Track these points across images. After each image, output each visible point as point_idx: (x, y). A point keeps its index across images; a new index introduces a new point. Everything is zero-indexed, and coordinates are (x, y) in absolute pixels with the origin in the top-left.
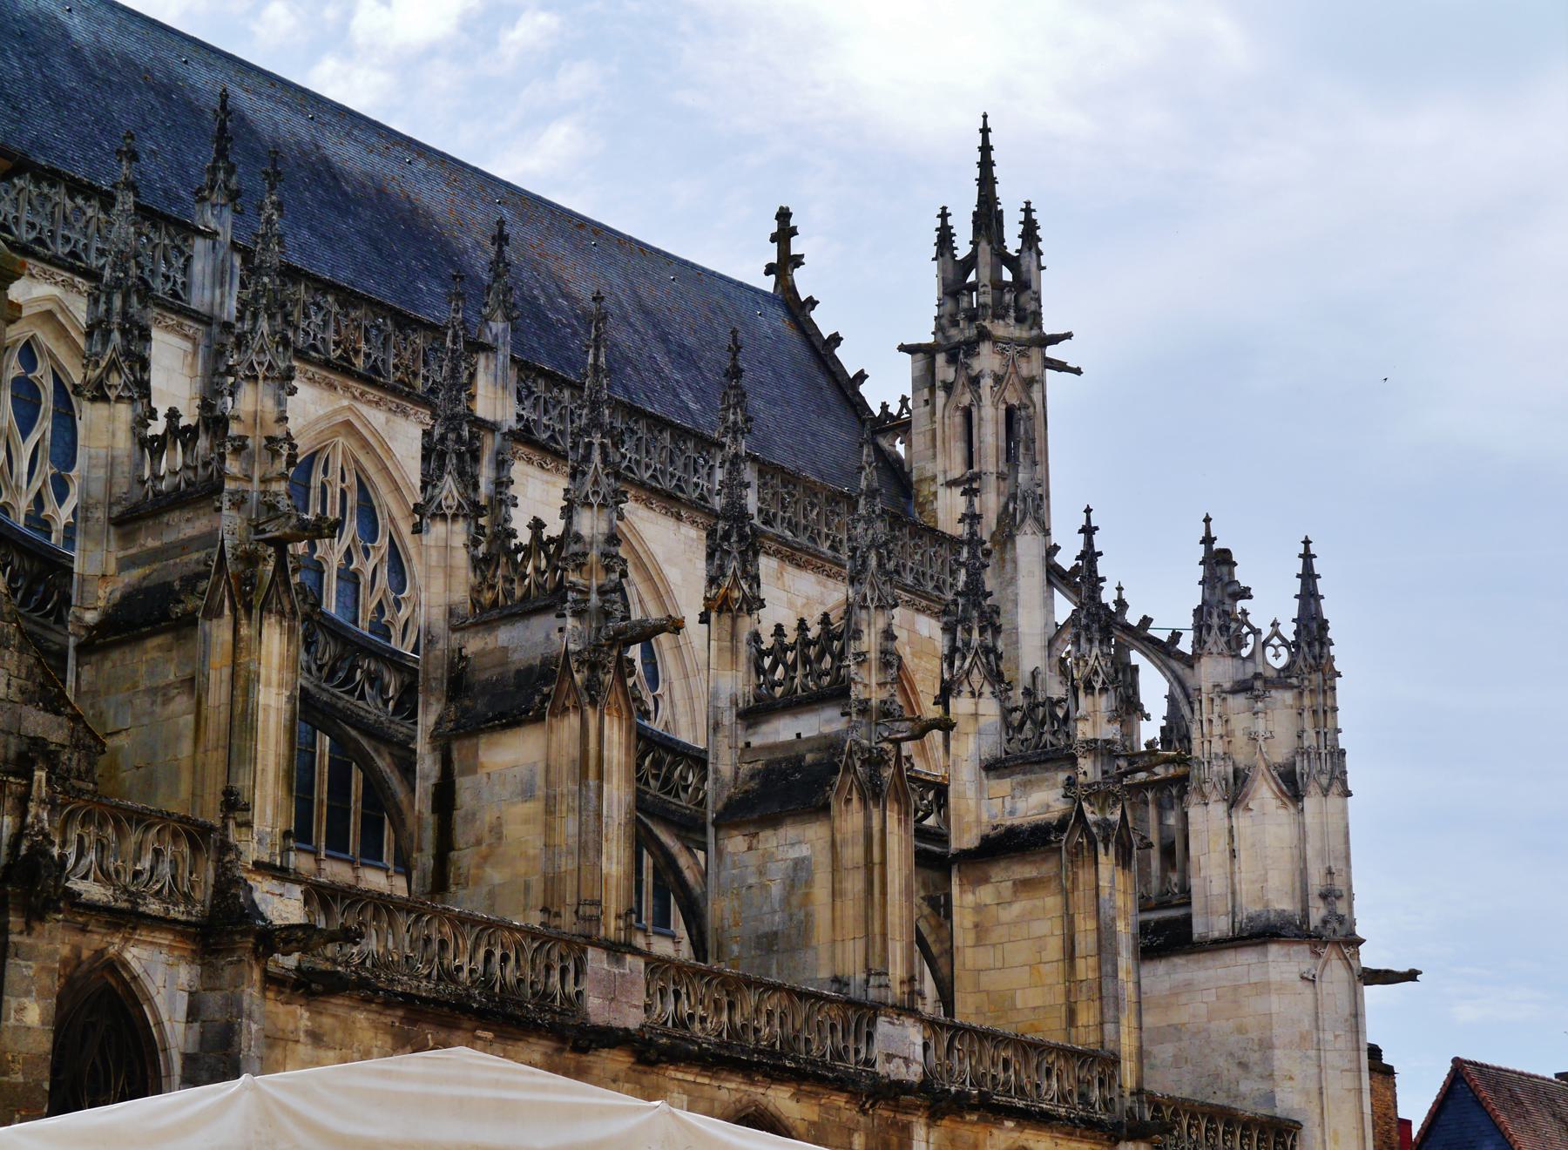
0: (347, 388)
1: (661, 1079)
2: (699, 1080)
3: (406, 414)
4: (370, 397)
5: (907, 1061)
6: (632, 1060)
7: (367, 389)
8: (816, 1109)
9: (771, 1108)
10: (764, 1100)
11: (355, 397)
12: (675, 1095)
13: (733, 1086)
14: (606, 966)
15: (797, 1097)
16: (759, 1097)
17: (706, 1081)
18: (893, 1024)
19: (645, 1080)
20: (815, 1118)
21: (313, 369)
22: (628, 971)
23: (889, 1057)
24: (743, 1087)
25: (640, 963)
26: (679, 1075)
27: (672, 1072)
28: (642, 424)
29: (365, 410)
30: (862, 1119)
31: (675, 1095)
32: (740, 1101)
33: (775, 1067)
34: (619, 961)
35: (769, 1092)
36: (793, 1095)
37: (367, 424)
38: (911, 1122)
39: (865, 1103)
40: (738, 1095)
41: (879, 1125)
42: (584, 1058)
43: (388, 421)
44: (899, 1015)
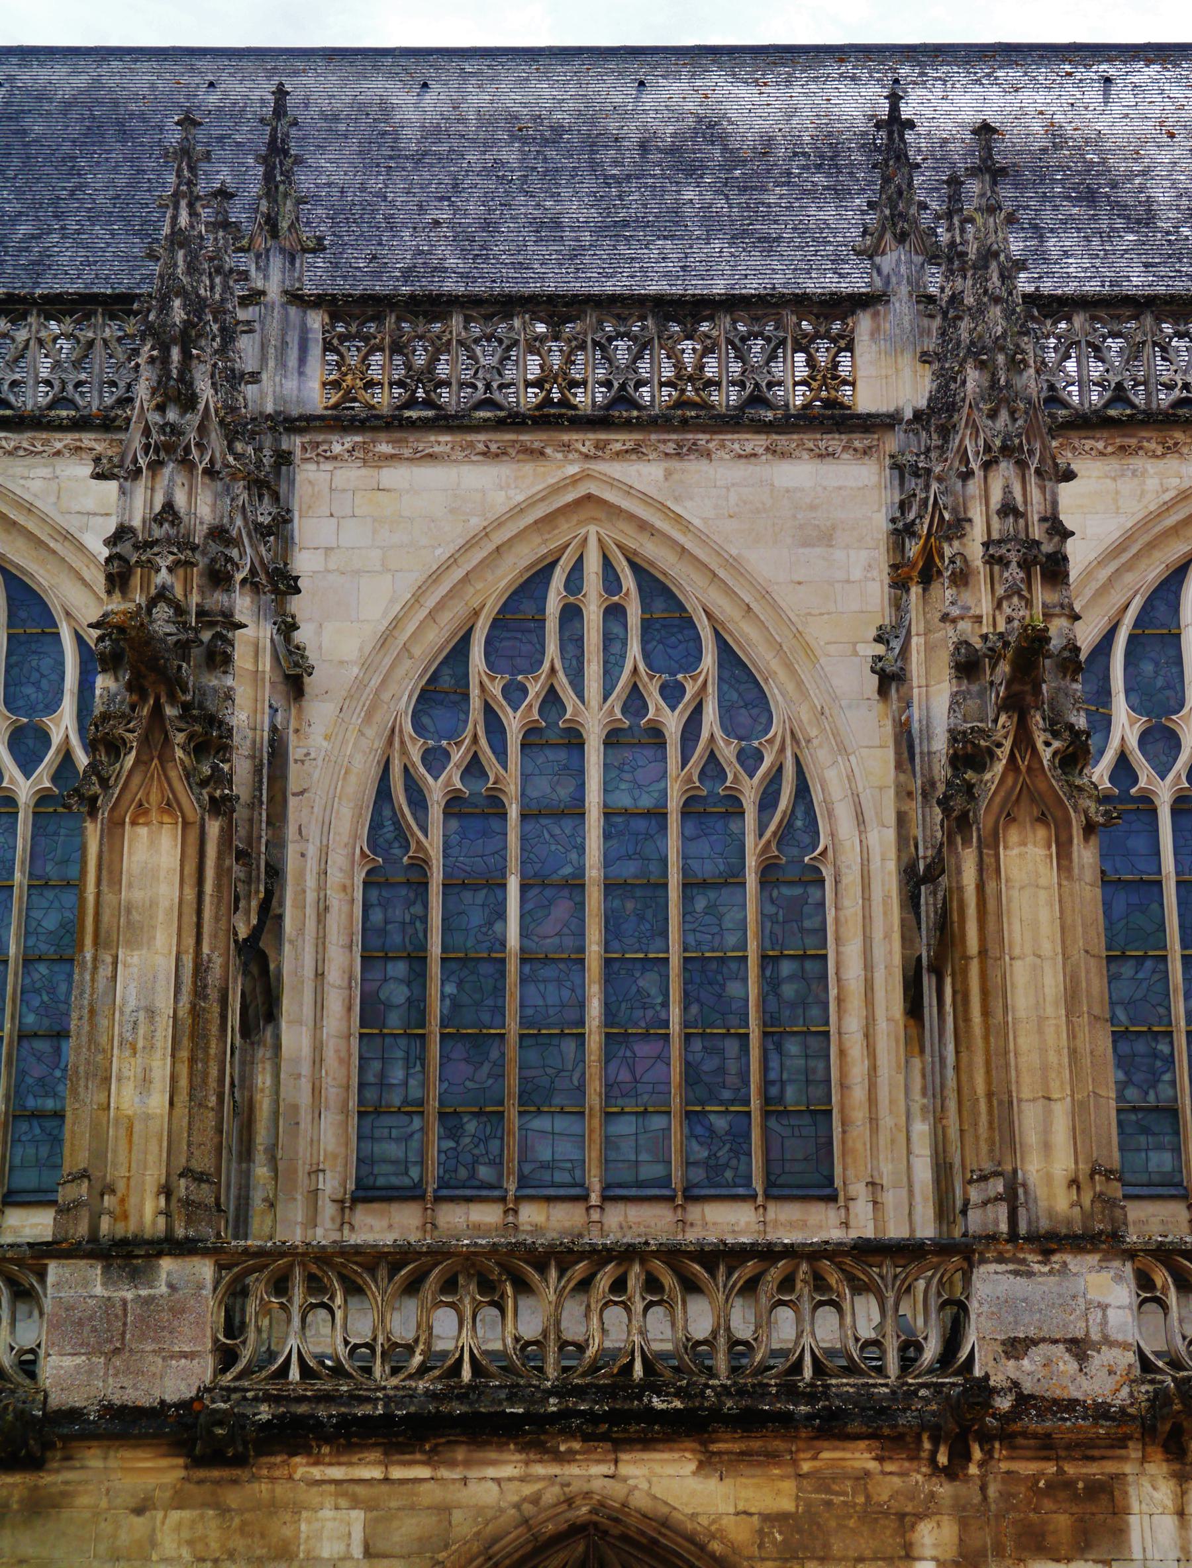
0: (567, 447)
1: (280, 1489)
2: (397, 1473)
3: (785, 455)
4: (618, 447)
5: (1079, 1348)
6: (181, 1461)
7: (603, 436)
8: (789, 1486)
9: (639, 1501)
10: (617, 1490)
11: (587, 457)
12: (327, 1513)
13: (507, 1471)
14: (99, 1290)
15: (708, 1463)
16: (597, 1485)
17: (423, 1472)
18: (1030, 1274)
19: (232, 1498)
20: (787, 1505)
21: (482, 437)
22: (164, 1289)
23: (1016, 1347)
24: (540, 1470)
25: (205, 1269)
26: (337, 1473)
27: (302, 1468)
28: (1079, 320)
29: (616, 470)
30: (945, 1490)
31: (327, 1513)
32: (535, 1500)
33: (615, 1417)
34: (136, 1276)
35: (624, 1470)
36: (701, 1465)
37: (629, 490)
38: (1120, 1477)
39: (934, 1453)
40: (528, 1490)
41: (1005, 1496)
42: (47, 1479)
43: (668, 474)
44: (1047, 1253)
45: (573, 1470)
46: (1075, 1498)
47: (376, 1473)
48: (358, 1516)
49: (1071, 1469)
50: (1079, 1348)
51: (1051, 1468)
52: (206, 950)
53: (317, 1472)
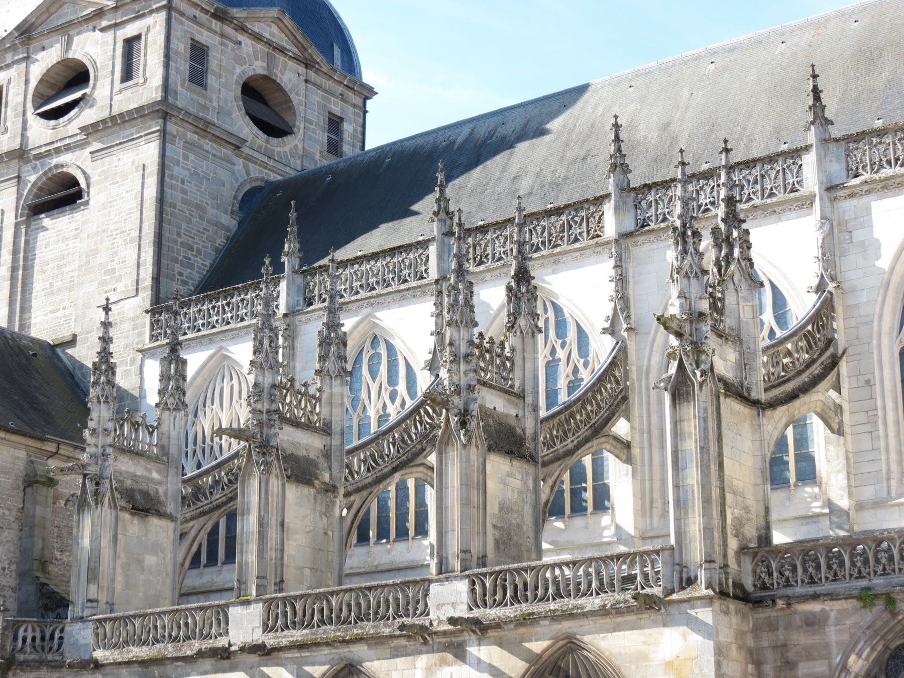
2: (303, 654)
5: (453, 605)
10: (351, 655)
16: (346, 654)
17: (308, 654)
23: (439, 606)
38: (465, 641)
40: (331, 657)
45: (341, 651)
46: (454, 648)
47: (298, 655)
48: (295, 666)
49: (454, 640)
50: (453, 605)
51: (449, 640)
52: (262, 513)
53: (286, 656)
